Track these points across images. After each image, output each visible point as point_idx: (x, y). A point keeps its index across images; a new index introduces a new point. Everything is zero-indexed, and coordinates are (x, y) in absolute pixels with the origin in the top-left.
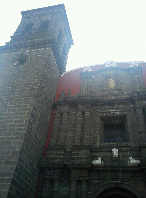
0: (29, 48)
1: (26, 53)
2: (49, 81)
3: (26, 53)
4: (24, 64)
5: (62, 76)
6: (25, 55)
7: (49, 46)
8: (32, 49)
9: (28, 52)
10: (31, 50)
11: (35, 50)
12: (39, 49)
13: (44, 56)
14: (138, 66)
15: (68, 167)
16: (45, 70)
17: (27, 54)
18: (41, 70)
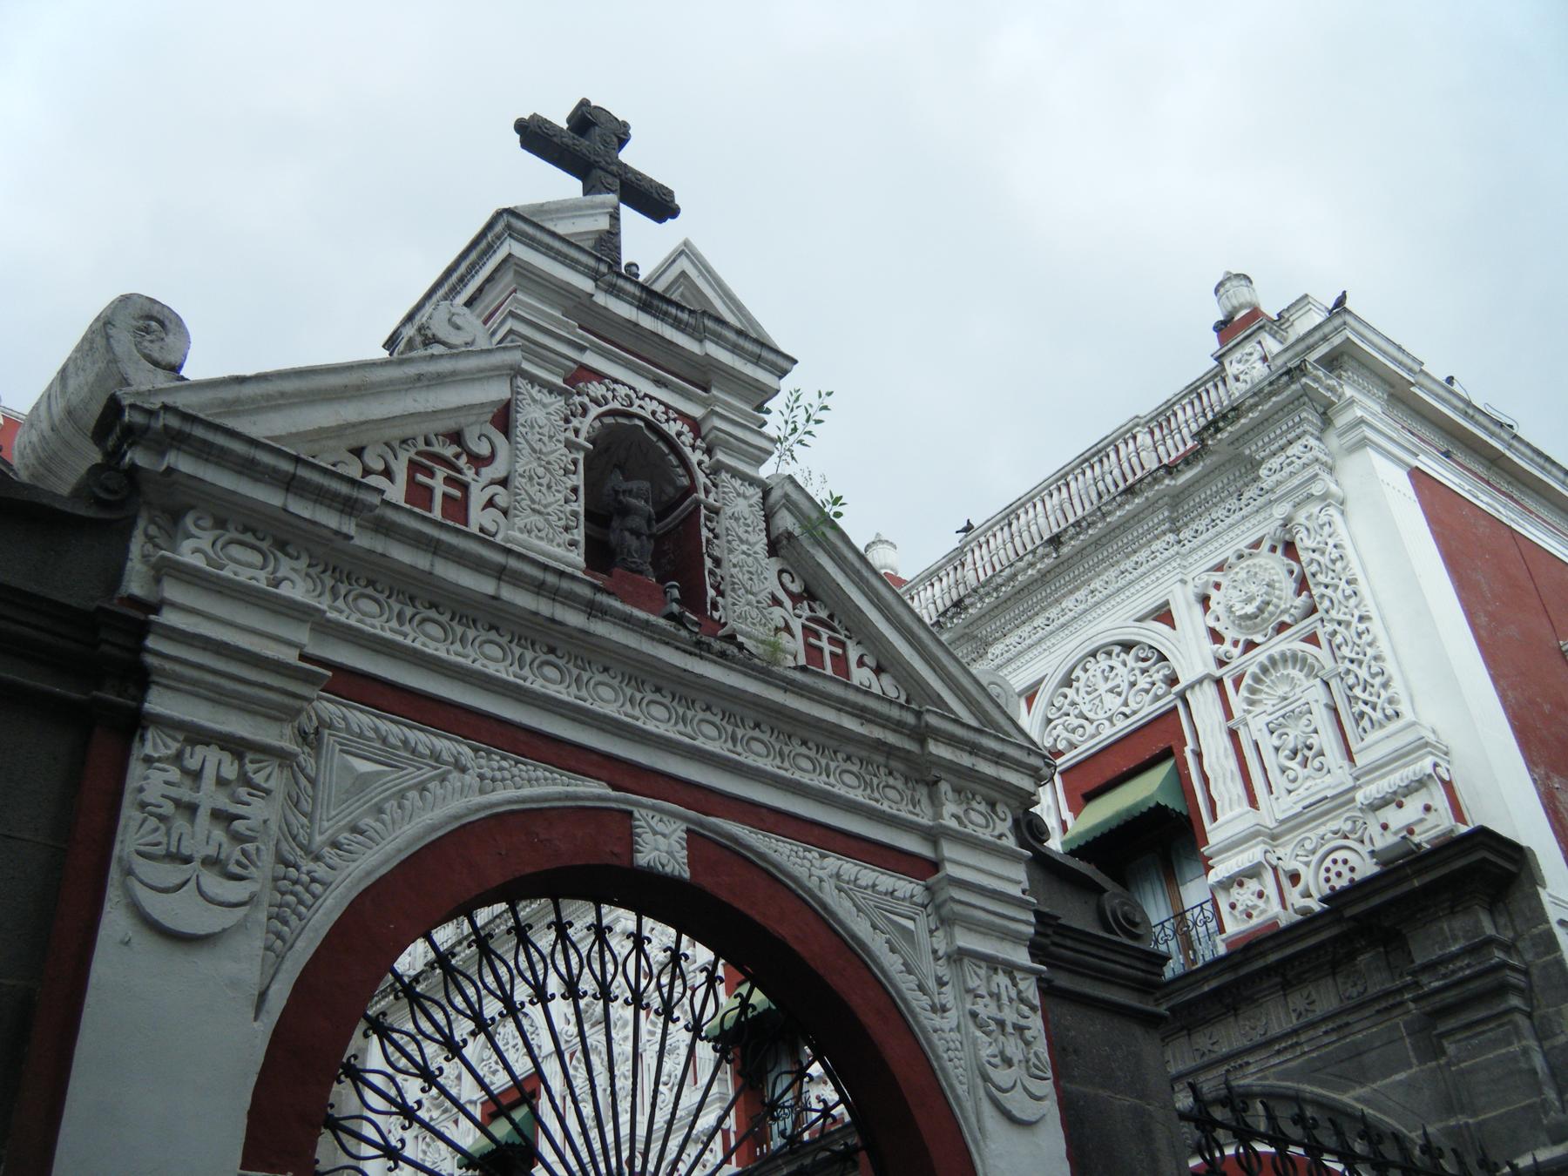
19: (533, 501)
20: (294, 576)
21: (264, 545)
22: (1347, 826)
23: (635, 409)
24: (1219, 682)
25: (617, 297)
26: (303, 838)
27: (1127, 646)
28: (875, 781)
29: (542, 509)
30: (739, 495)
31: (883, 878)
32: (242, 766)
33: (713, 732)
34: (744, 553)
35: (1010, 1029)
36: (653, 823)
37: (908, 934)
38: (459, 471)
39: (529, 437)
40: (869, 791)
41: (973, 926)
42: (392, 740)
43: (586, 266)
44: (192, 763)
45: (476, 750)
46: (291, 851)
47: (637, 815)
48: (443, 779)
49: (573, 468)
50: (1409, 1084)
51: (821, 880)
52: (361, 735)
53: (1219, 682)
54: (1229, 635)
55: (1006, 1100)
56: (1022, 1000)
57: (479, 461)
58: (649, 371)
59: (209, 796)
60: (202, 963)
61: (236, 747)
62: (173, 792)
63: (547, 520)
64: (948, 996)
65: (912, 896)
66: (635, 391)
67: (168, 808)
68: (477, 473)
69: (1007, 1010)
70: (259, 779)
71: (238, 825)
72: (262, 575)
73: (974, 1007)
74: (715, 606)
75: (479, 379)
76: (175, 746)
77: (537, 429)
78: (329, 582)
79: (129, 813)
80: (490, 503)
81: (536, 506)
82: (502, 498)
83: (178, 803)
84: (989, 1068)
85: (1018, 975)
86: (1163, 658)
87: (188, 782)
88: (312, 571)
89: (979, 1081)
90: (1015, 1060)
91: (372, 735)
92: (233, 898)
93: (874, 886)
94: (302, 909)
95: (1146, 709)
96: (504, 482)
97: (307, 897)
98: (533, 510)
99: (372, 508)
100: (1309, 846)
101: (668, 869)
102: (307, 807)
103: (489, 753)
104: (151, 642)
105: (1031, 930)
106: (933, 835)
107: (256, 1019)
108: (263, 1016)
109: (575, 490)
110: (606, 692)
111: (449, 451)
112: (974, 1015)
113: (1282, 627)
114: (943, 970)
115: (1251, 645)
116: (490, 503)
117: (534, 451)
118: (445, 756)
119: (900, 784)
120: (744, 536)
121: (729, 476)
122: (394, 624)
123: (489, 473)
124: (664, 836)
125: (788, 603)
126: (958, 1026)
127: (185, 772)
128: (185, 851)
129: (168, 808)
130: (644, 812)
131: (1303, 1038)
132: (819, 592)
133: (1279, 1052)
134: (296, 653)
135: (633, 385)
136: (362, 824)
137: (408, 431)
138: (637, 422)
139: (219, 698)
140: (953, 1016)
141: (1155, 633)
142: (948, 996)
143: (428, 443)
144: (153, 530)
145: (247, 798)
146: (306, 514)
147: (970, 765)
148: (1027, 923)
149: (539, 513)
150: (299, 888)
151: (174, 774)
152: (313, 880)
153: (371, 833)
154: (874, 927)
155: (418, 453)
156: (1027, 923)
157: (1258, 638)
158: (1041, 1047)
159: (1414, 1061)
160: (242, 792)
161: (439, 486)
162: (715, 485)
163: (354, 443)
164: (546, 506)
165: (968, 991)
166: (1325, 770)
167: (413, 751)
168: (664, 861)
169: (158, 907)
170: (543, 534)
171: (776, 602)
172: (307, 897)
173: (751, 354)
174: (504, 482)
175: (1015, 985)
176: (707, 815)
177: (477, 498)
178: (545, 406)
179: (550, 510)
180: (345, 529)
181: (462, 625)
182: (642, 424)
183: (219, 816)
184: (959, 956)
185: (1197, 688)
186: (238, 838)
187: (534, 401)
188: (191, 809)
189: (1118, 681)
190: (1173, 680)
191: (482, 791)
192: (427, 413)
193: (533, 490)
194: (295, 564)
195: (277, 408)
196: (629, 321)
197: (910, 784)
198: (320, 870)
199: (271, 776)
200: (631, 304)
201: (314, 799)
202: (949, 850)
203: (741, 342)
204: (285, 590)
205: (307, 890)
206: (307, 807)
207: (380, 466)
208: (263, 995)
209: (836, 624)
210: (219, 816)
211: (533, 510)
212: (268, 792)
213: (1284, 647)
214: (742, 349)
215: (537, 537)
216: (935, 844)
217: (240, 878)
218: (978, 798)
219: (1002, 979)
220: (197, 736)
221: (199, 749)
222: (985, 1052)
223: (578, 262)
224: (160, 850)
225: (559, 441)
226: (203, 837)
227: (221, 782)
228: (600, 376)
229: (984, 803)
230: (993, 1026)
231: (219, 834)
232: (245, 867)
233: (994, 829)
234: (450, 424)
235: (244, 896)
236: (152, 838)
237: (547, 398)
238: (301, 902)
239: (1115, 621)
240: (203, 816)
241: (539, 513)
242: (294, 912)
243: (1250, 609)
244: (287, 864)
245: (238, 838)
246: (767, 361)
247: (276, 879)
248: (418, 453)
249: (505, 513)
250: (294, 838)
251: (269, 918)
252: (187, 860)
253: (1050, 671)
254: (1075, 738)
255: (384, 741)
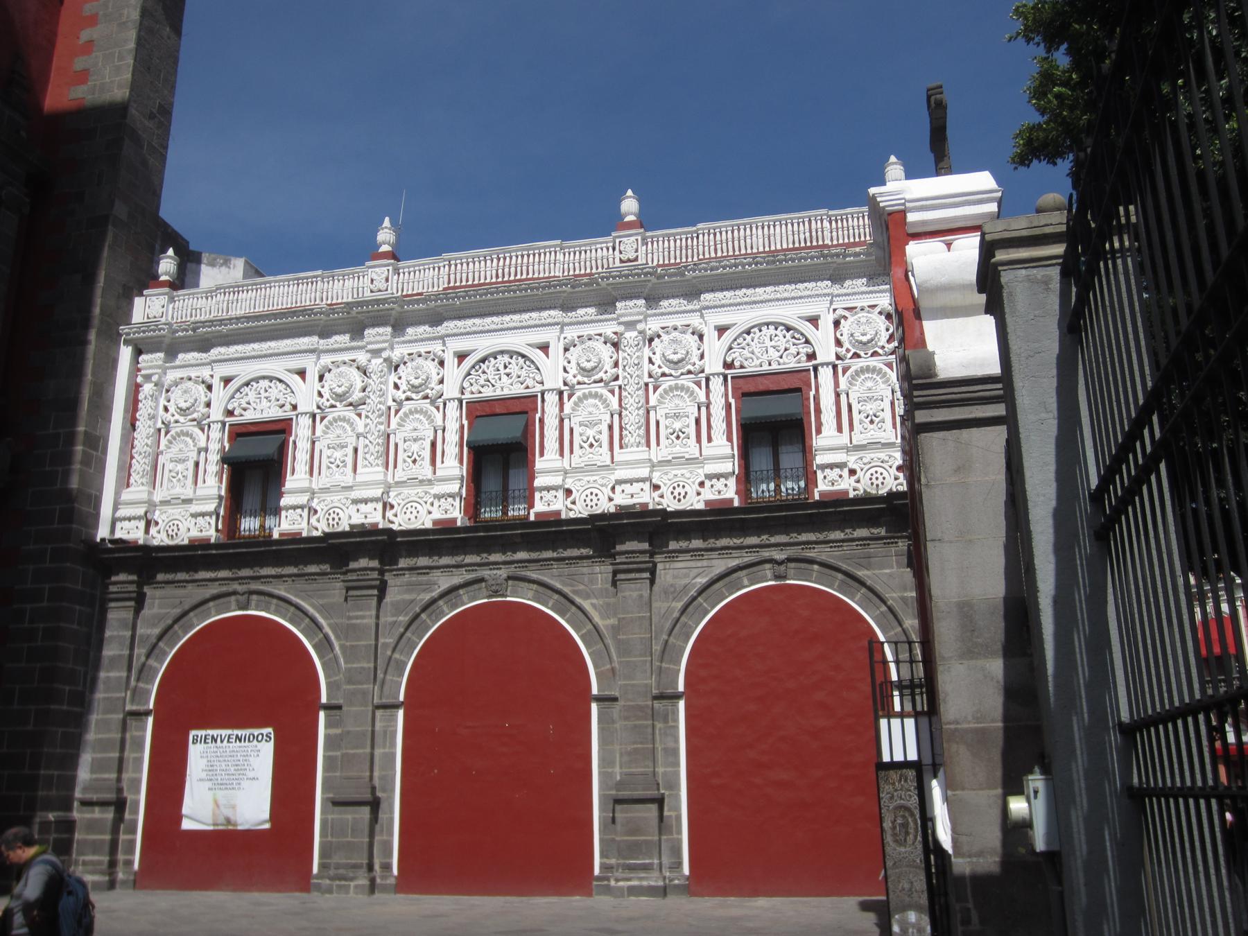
22: (886, 459)
24: (835, 367)
27: (788, 329)
50: (890, 575)
53: (835, 367)
54: (847, 345)
86: (807, 342)
95: (790, 363)
100: (865, 460)
113: (875, 354)
115: (856, 355)
131: (845, 544)
133: (831, 547)
141: (807, 328)
157: (862, 354)
159: (895, 566)
166: (883, 429)
185: (825, 367)
189: (779, 343)
190: (812, 356)
213: (875, 364)
239: (790, 313)
243: (864, 339)
253: (739, 323)
254: (746, 364)
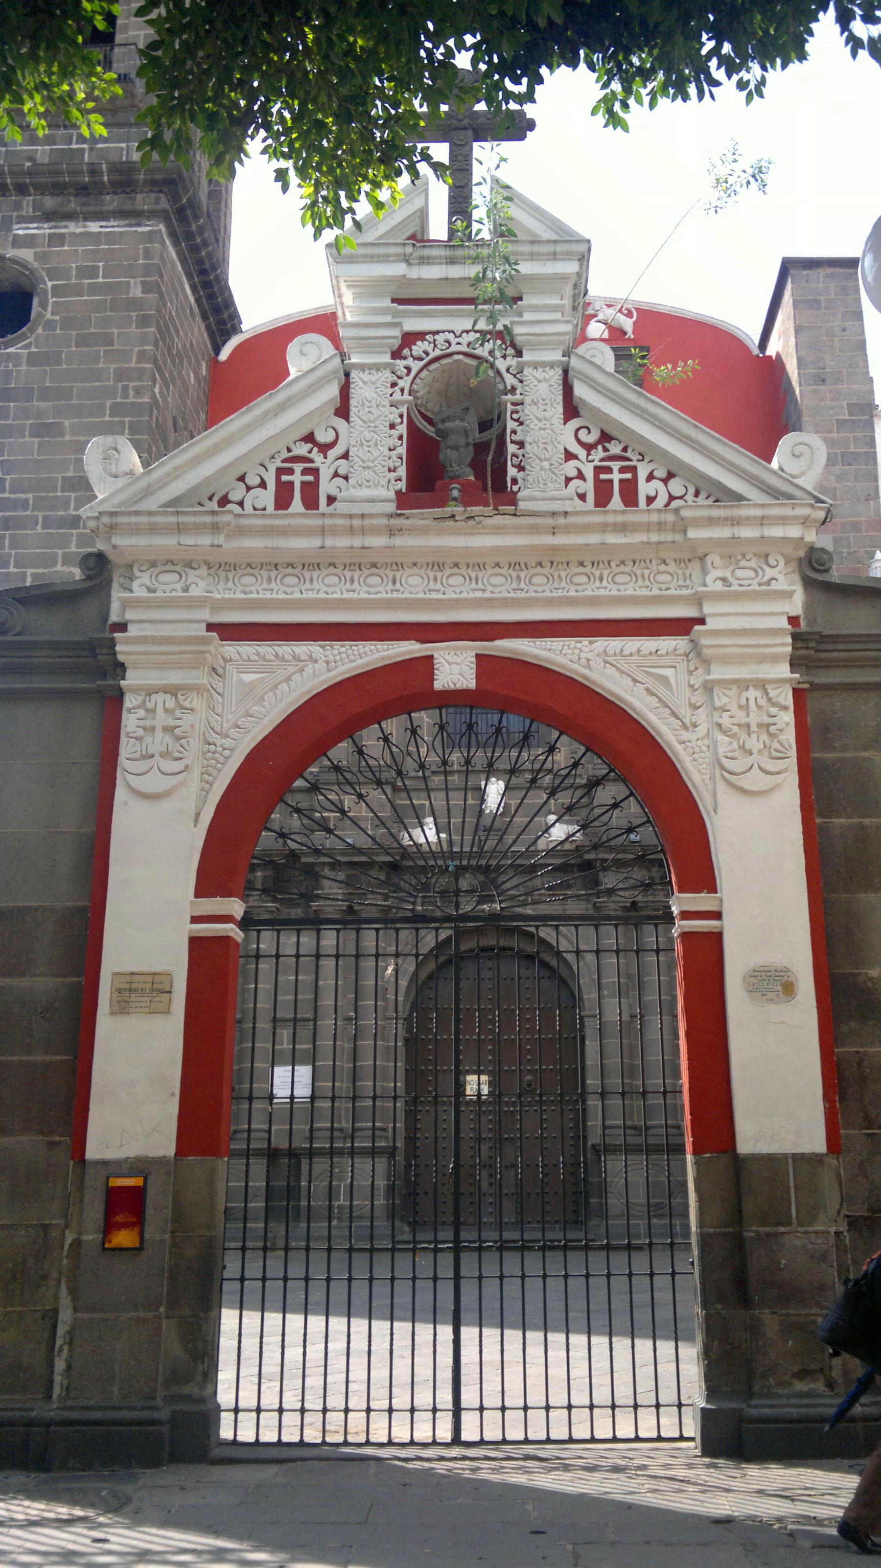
0: (28, 203)
1: (18, 242)
2: (176, 431)
3: (18, 242)
4: (24, 337)
5: (224, 355)
6: (13, 261)
7: (152, 214)
8: (49, 216)
9: (29, 242)
10: (45, 230)
11: (73, 228)
12: (94, 227)
13: (136, 292)
14: (630, 334)
15: (303, 860)
16: (157, 390)
17: (26, 254)
18: (138, 392)
19: (364, 461)
20: (198, 580)
21: (178, 568)
23: (454, 348)
25: (428, 263)
26: (218, 728)
28: (647, 572)
29: (370, 464)
30: (540, 381)
31: (647, 644)
32: (176, 697)
33: (500, 580)
34: (541, 429)
35: (754, 728)
36: (447, 657)
37: (665, 680)
38: (312, 461)
39: (360, 414)
40: (640, 582)
41: (726, 660)
42: (268, 657)
43: (396, 255)
44: (150, 705)
45: (322, 647)
46: (213, 737)
47: (436, 656)
48: (301, 670)
49: (399, 420)
51: (588, 660)
52: (249, 660)
55: (745, 782)
56: (774, 705)
57: (324, 448)
58: (463, 310)
59: (162, 719)
60: (166, 805)
61: (172, 691)
62: (141, 723)
63: (374, 472)
64: (701, 715)
65: (675, 650)
66: (453, 332)
67: (140, 732)
68: (325, 457)
69: (752, 715)
70: (187, 704)
71: (177, 731)
72: (178, 586)
73: (720, 721)
74: (515, 481)
75: (314, 391)
76: (140, 699)
77: (367, 404)
78: (222, 575)
79: (123, 739)
80: (336, 475)
81: (366, 465)
82: (343, 467)
83: (144, 729)
84: (725, 761)
85: (769, 688)
87: (150, 716)
88: (212, 571)
89: (718, 772)
90: (755, 751)
91: (256, 658)
92: (177, 770)
93: (639, 651)
94: (219, 766)
96: (346, 456)
97: (222, 759)
98: (364, 468)
99: (229, 524)
101: (459, 686)
102: (219, 710)
103: (332, 646)
104: (118, 648)
105: (789, 649)
106: (698, 600)
107: (195, 826)
108: (199, 825)
109: (401, 438)
110: (415, 580)
111: (302, 449)
112: (719, 726)
114: (698, 698)
116: (336, 475)
117: (365, 422)
118: (303, 657)
119: (672, 568)
120: (541, 415)
121: (530, 370)
122: (265, 585)
123: (332, 453)
124: (457, 664)
125: (582, 453)
126: (708, 734)
127: (147, 710)
128: (150, 752)
129: (140, 732)
130: (442, 653)
132: (613, 433)
134: (204, 626)
135: (450, 328)
136: (251, 712)
137: (273, 450)
138: (456, 357)
139: (161, 666)
140: (702, 730)
142: (701, 715)
143: (289, 450)
144: (122, 580)
145: (180, 715)
146: (191, 542)
147: (730, 535)
148: (784, 645)
149: (369, 468)
150: (217, 755)
151: (141, 713)
152: (224, 749)
153: (257, 714)
154: (635, 681)
155: (284, 461)
156: (784, 645)
158: (790, 736)
160: (178, 713)
161: (297, 479)
162: (521, 381)
163: (239, 473)
164: (373, 462)
165: (715, 709)
167: (283, 659)
168: (455, 681)
169: (136, 782)
170: (371, 483)
171: (569, 456)
172: (222, 759)
173: (548, 254)
174: (346, 456)
175: (767, 694)
176: (492, 639)
177: (325, 474)
178: (373, 383)
179: (376, 463)
180: (216, 542)
181: (309, 570)
182: (460, 357)
183: (167, 729)
184: (709, 687)
186: (178, 739)
187: (365, 383)
188: (153, 729)
191: (329, 670)
192: (277, 434)
193: (361, 454)
194: (197, 572)
195: (177, 478)
196: (440, 279)
197: (683, 564)
198: (227, 742)
199: (195, 701)
200: (441, 263)
201: (223, 704)
202: (708, 609)
203: (536, 248)
204: (194, 592)
205: (221, 754)
206: (219, 710)
207: (258, 481)
208: (198, 815)
209: (629, 454)
210: (167, 729)
211: (364, 468)
212: (192, 710)
214: (539, 254)
215: (367, 487)
216: (700, 605)
217: (181, 759)
218: (748, 557)
219: (753, 694)
220: (151, 691)
221: (154, 697)
222: (721, 751)
223: (388, 255)
224: (138, 755)
225: (384, 406)
226: (159, 741)
227: (167, 711)
228: (421, 336)
229: (754, 560)
230: (736, 729)
231: (168, 739)
232: (181, 753)
233: (763, 576)
234: (304, 431)
235: (181, 768)
236: (133, 750)
237: (375, 376)
238: (218, 762)
240: (159, 733)
241: (369, 468)
242: (215, 768)
244: (210, 744)
245: (178, 739)
246: (563, 253)
247: (204, 753)
248: (284, 461)
249: (346, 478)
250: (212, 729)
251: (202, 774)
252: (152, 756)
255: (264, 659)
